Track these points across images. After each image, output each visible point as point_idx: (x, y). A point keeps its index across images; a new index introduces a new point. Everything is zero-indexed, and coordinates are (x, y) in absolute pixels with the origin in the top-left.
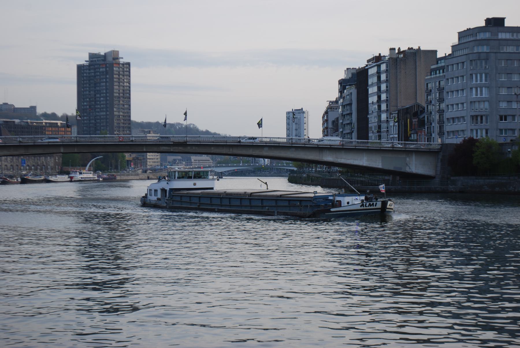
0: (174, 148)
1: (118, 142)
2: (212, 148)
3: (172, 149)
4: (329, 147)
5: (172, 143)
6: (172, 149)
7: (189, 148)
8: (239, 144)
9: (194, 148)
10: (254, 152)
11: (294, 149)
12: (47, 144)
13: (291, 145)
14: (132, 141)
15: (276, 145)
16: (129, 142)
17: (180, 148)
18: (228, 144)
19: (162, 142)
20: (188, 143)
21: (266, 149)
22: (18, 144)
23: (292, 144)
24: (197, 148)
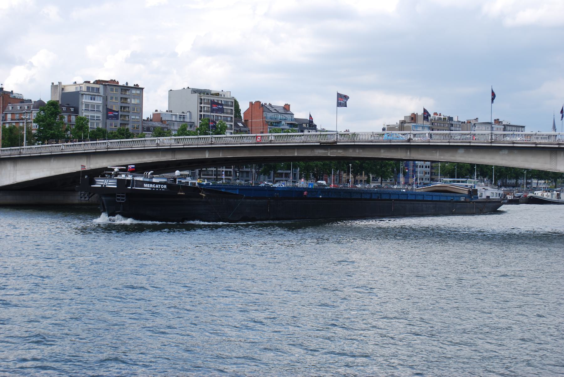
0: (331, 151)
1: (256, 143)
2: (382, 151)
3: (329, 153)
4: (557, 146)
5: (319, 144)
6: (329, 153)
7: (351, 151)
8: (409, 144)
9: (357, 151)
10: (442, 157)
11: (506, 152)
12: (183, 147)
13: (490, 145)
14: (271, 142)
15: (465, 144)
16: (267, 143)
17: (339, 151)
18: (392, 144)
19: (305, 143)
20: (338, 144)
21: (461, 151)
22: (156, 148)
23: (491, 143)
24: (361, 151)
